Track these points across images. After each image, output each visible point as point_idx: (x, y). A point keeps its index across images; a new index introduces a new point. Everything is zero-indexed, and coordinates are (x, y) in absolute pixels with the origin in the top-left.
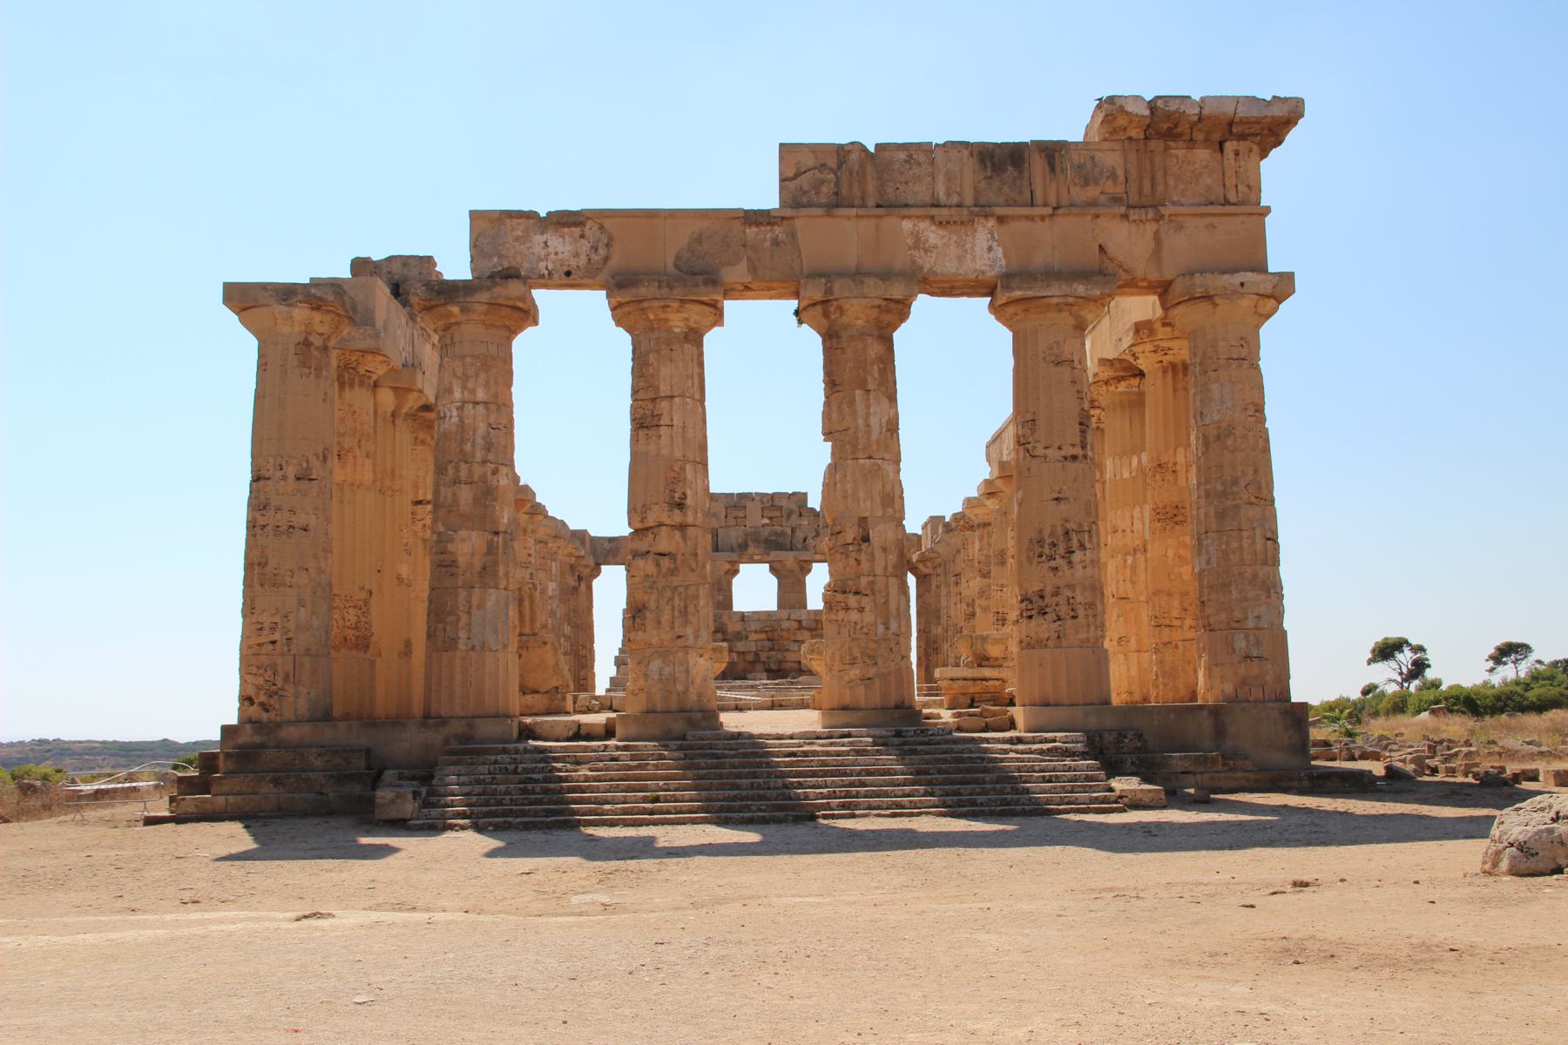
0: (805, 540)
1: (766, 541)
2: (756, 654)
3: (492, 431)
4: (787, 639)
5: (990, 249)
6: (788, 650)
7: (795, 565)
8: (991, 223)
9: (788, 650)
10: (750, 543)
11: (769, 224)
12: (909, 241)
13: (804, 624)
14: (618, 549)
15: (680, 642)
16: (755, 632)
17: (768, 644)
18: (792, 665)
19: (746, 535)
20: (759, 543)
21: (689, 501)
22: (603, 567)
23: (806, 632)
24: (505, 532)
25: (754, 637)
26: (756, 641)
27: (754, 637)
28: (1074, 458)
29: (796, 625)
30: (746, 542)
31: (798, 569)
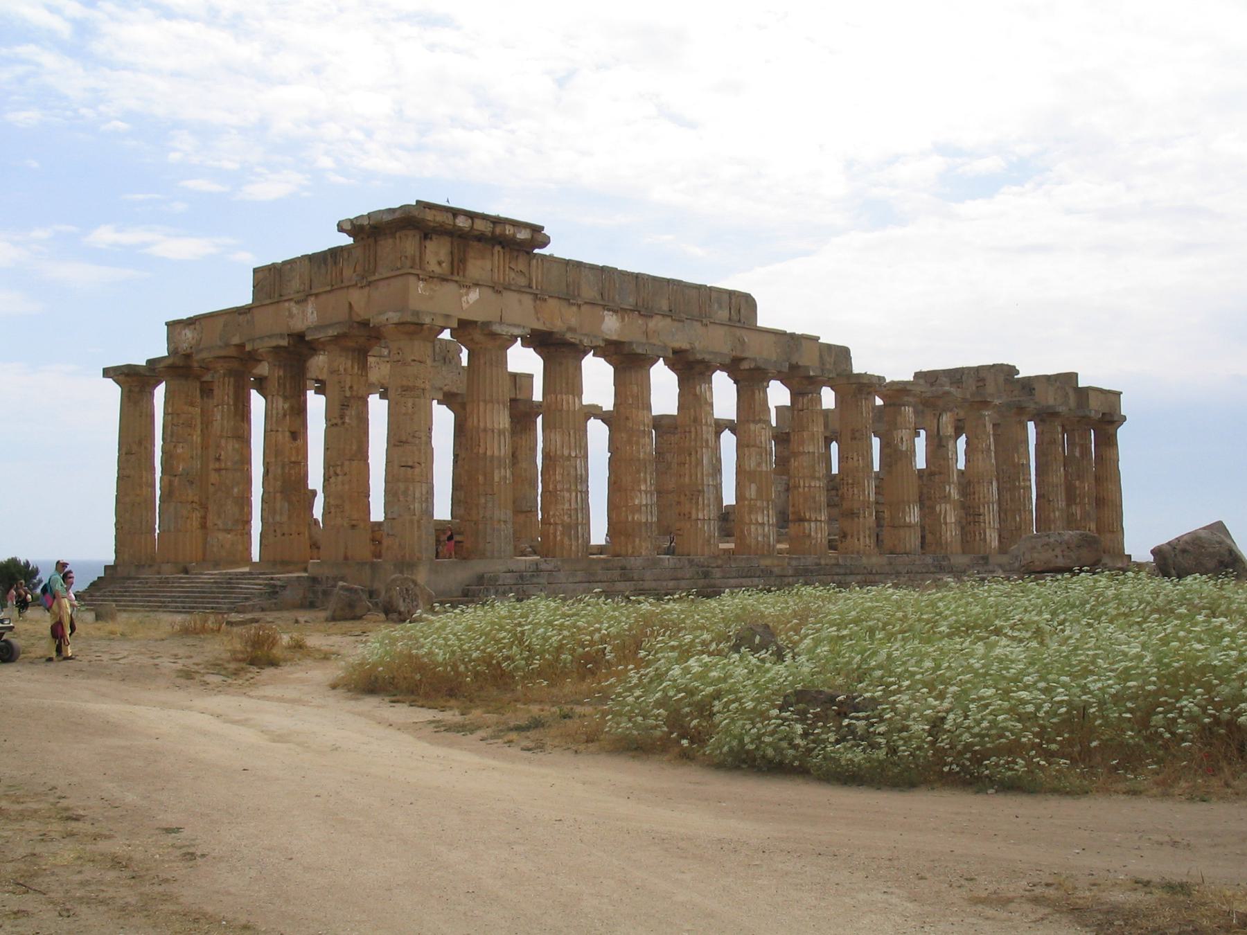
3: (175, 428)
5: (312, 313)
8: (313, 298)
11: (245, 313)
12: (287, 314)
15: (216, 527)
21: (222, 457)
24: (181, 475)
28: (336, 424)
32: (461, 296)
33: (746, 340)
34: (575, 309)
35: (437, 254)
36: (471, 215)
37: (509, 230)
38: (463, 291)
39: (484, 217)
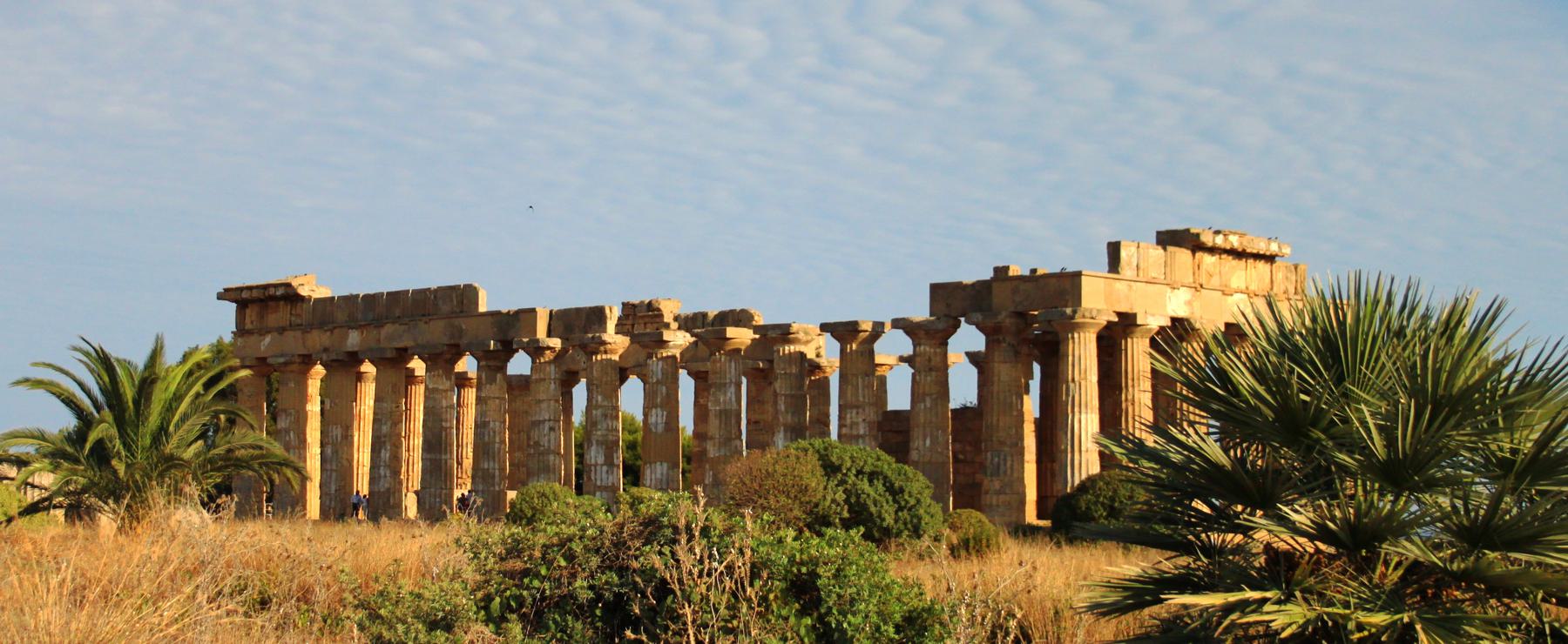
32: (261, 341)
33: (464, 327)
34: (328, 333)
35: (251, 313)
36: (250, 288)
37: (272, 291)
38: (262, 338)
39: (257, 287)
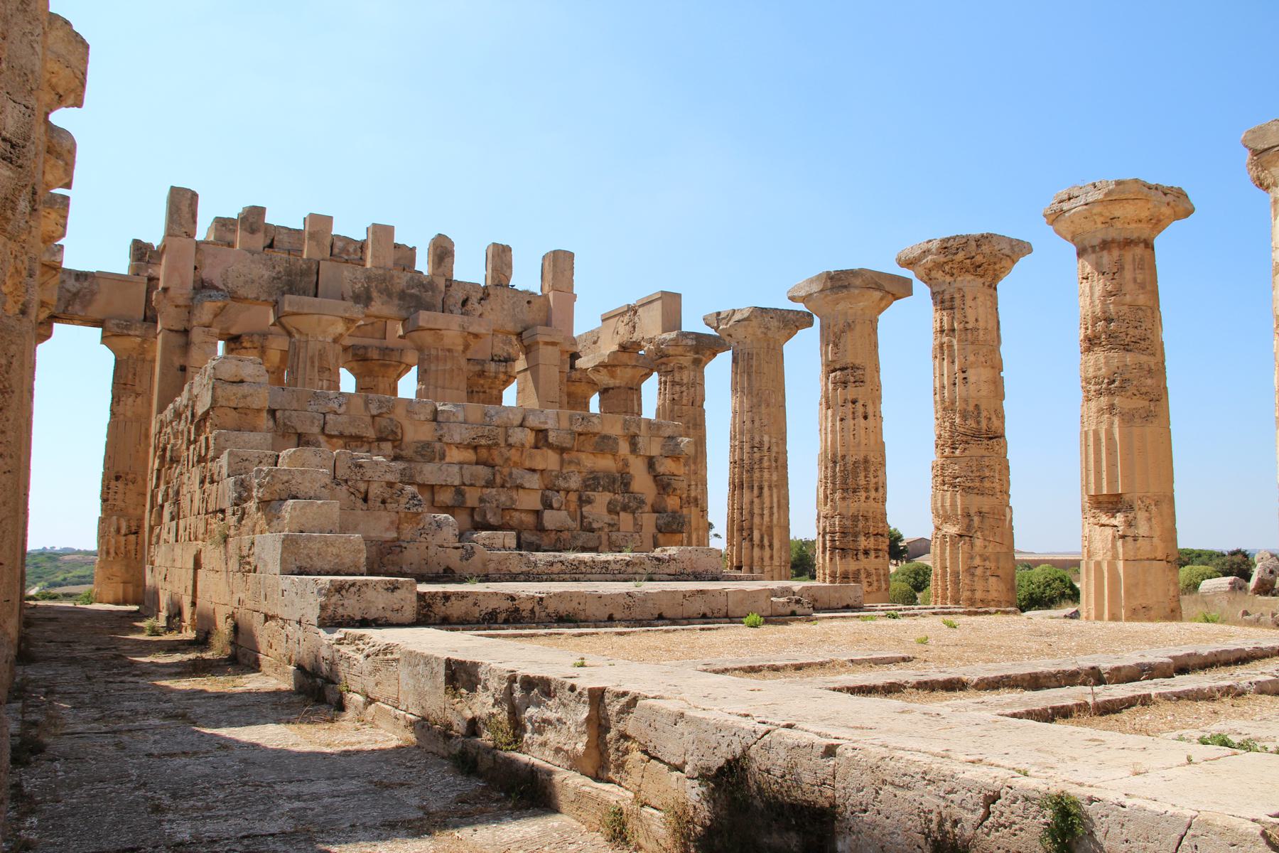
0: (465, 303)
1: (403, 295)
2: (459, 491)
4: (516, 464)
6: (520, 487)
7: (460, 341)
9: (520, 487)
10: (375, 294)
13: (552, 437)
14: (93, 293)
16: (458, 446)
17: (483, 471)
18: (525, 517)
19: (369, 278)
20: (390, 295)
22: (58, 327)
23: (550, 452)
25: (455, 455)
26: (461, 463)
27: (455, 455)
29: (529, 438)
30: (367, 290)
31: (461, 348)
